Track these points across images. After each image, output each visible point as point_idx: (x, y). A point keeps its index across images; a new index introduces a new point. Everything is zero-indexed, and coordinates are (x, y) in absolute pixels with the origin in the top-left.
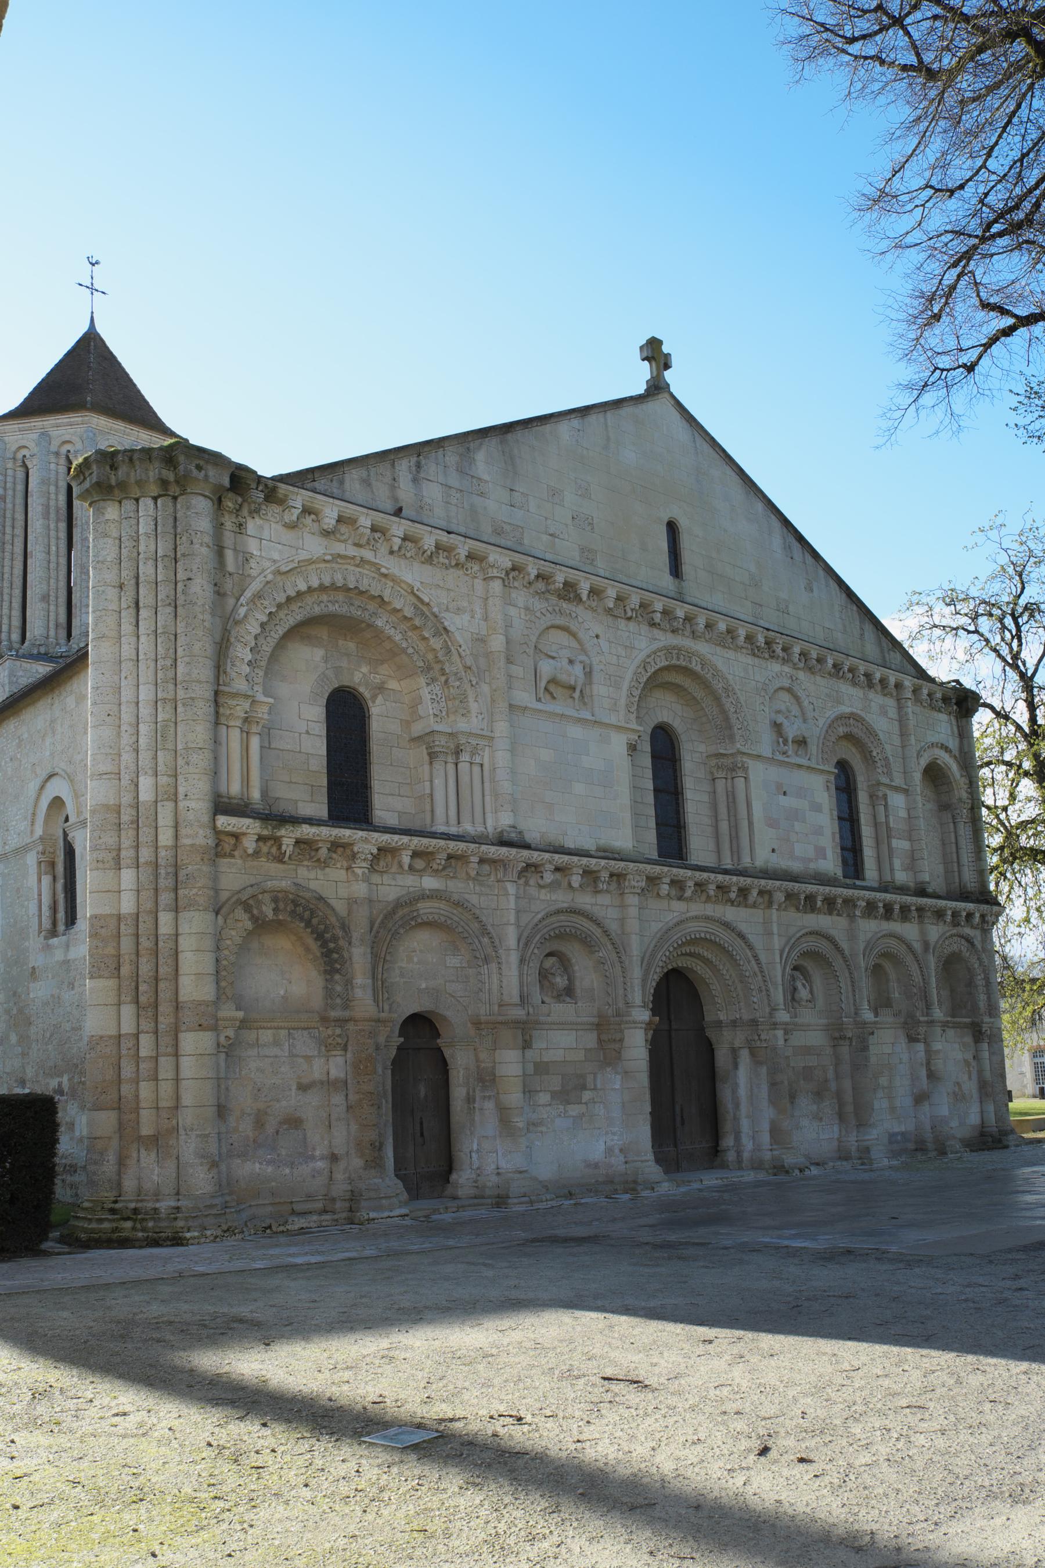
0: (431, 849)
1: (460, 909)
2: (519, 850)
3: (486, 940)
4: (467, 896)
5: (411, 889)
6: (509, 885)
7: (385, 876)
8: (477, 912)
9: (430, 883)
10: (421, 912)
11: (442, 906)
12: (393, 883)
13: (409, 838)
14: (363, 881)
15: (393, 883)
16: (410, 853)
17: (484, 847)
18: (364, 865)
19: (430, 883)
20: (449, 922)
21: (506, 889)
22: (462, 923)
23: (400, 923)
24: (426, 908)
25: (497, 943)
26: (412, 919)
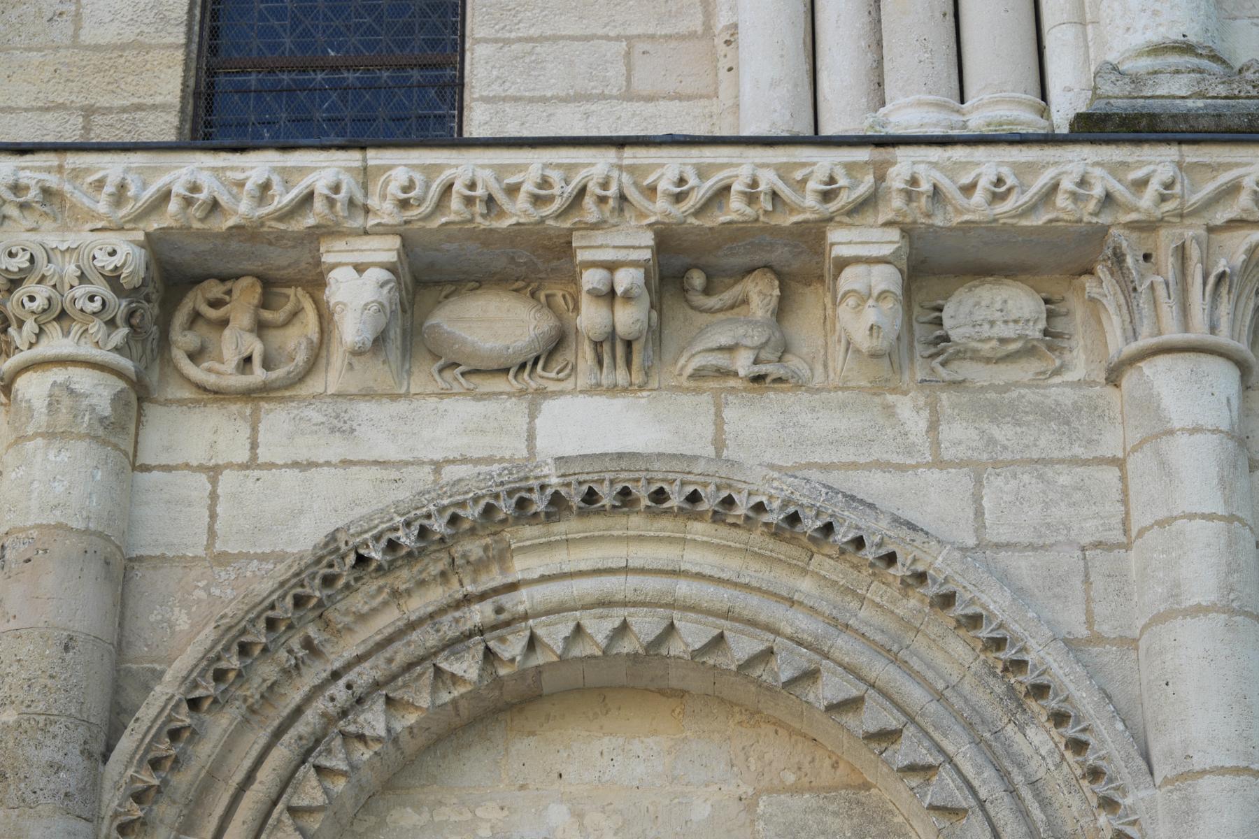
0: (518, 211)
1: (823, 563)
2: (1193, 154)
3: (1037, 741)
4: (872, 485)
5: (451, 473)
6: (1162, 377)
7: (277, 421)
8: (939, 562)
9: (585, 424)
10: (523, 600)
11: (694, 559)
12: (336, 449)
13: (353, 158)
14: (50, 435)
15: (336, 449)
16: (386, 250)
17: (905, 162)
18: (57, 343)
19: (585, 424)
20: (743, 646)
21: (1150, 405)
22: (843, 645)
23: (364, 675)
24: (561, 581)
25: (1109, 742)
26: (452, 645)
